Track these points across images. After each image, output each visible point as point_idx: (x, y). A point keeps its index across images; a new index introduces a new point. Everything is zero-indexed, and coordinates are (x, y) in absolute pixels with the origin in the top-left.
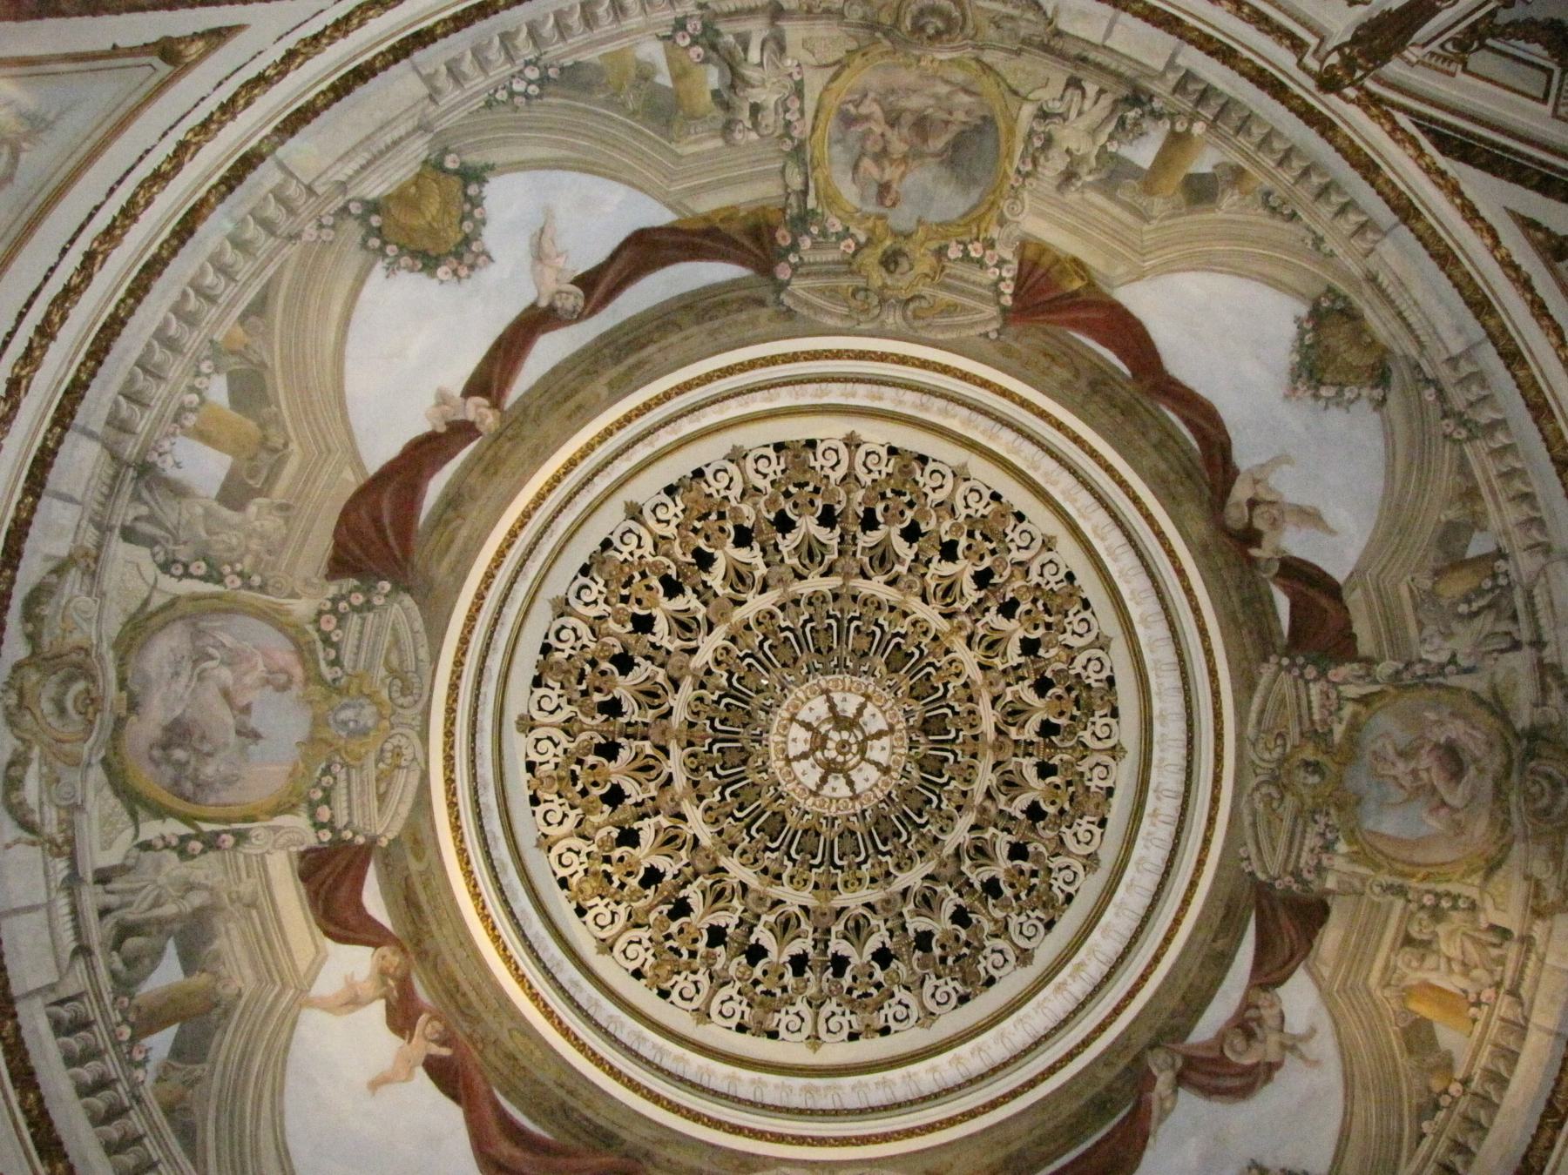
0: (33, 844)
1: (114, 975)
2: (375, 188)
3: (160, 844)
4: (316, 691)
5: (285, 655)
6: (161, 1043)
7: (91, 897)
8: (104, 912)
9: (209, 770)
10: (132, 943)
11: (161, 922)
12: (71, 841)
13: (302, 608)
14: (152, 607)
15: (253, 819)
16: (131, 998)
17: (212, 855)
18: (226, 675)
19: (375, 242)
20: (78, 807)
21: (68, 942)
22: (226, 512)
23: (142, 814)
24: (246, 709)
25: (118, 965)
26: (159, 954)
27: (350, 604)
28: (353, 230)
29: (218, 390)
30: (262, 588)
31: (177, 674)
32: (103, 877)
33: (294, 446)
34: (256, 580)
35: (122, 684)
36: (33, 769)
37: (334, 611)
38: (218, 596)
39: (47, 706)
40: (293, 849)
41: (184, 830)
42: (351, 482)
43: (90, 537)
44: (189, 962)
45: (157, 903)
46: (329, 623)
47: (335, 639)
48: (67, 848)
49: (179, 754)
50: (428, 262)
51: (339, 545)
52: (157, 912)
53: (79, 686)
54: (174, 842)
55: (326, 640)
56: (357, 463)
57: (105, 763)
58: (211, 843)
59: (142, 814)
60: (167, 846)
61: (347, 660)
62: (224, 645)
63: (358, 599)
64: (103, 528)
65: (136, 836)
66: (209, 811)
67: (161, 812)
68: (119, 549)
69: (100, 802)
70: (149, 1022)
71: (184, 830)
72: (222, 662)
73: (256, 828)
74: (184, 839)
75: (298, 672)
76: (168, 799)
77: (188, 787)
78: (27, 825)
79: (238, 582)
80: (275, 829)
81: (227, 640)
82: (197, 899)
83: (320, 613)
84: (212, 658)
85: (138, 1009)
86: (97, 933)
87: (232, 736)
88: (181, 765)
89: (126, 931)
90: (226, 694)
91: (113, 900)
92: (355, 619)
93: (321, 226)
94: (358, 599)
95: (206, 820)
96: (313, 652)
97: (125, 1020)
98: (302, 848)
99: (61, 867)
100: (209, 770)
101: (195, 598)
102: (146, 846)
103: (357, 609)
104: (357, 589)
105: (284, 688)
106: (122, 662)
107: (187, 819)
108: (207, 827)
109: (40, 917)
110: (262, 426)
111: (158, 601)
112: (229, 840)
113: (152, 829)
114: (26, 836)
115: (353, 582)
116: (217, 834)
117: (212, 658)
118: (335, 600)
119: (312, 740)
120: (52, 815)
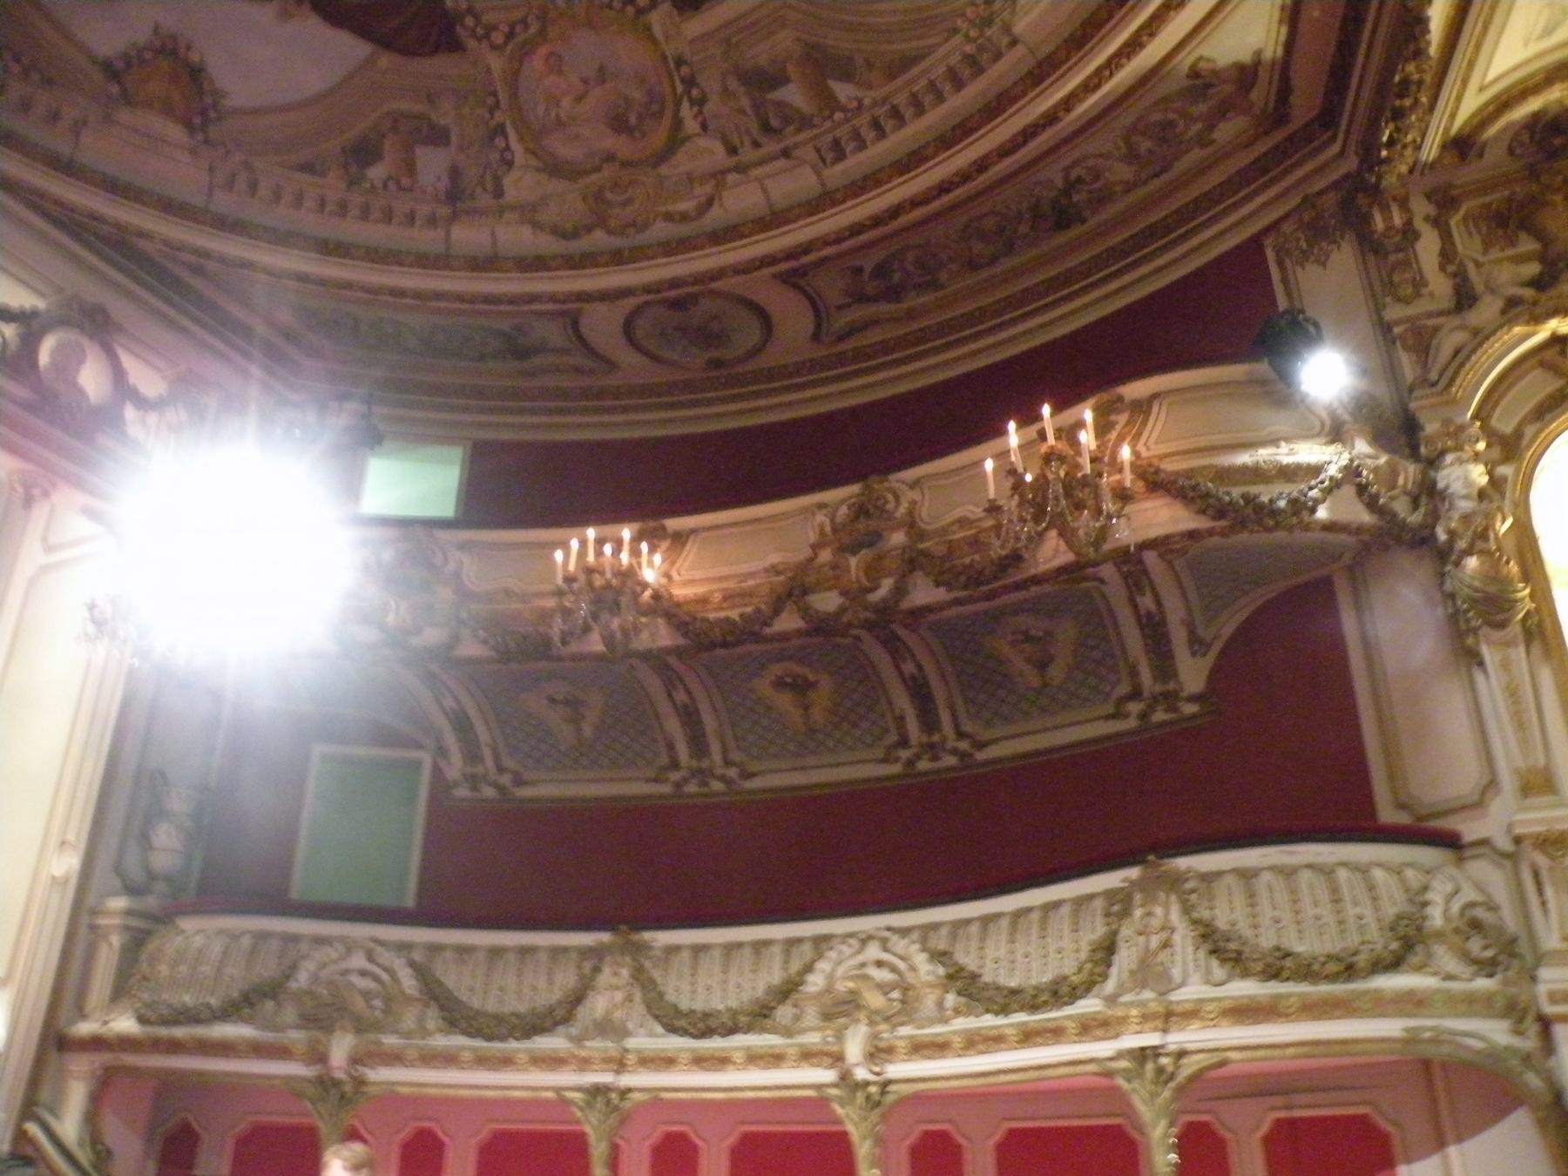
0: (720, 199)
1: (799, 130)
2: (176, 132)
3: (700, 119)
4: (552, 32)
5: (536, 63)
6: (843, 91)
7: (748, 154)
8: (756, 145)
9: (637, 95)
10: (774, 122)
11: (756, 107)
12: (713, 175)
13: (496, 63)
14: (541, 165)
15: (664, 58)
16: (813, 115)
17: (700, 79)
18: (566, 102)
19: (213, 114)
20: (690, 178)
21: (781, 163)
22: (454, 138)
23: (681, 135)
24: (585, 81)
25: (791, 128)
26: (780, 105)
27: (476, 25)
28: (213, 132)
29: (376, 173)
30: (494, 94)
31: (577, 136)
32: (732, 150)
33: (385, 108)
34: (490, 100)
35: (598, 169)
36: (670, 208)
37: (487, 36)
38: (514, 124)
39: (629, 209)
40: (677, 19)
41: (686, 104)
42: (385, 60)
43: (508, 216)
44: (780, 80)
45: (742, 111)
46: (498, 38)
47: (506, 29)
48: (718, 176)
49: (633, 120)
50: (196, 73)
51: (435, 51)
52: (749, 111)
53: (609, 195)
54: (696, 109)
55: (510, 35)
56: (369, 62)
57: (655, 166)
58: (690, 82)
59: (681, 135)
60: (700, 112)
61: (517, 15)
62: (546, 110)
63: (469, 21)
64: (501, 211)
65: (698, 135)
66: (668, 90)
67: (678, 124)
68: (511, 193)
69: (682, 162)
70: (829, 102)
71: (686, 104)
72: (558, 105)
73: (670, 50)
74: (692, 102)
75: (543, 50)
76: (667, 121)
77: (655, 108)
78: (710, 203)
79: (498, 114)
80: (667, 37)
81: (540, 110)
82: (733, 84)
83: (493, 47)
84: (558, 116)
85: (820, 110)
86: (771, 147)
87: (608, 86)
88: (640, 118)
89: (767, 128)
90: (580, 98)
91: (747, 142)
92: (487, 18)
93: (228, 152)
94: (469, 21)
95: (674, 88)
96: (524, 43)
97: (830, 117)
98: (675, 12)
99: (732, 178)
100: (637, 95)
101: (521, 139)
102: (704, 127)
103: (477, 17)
104: (462, 24)
105: (560, 58)
106: (587, 173)
107: (678, 104)
108: (680, 88)
109: (768, 183)
110: (384, 136)
111: (533, 162)
112: (685, 70)
113: (691, 125)
114: (716, 202)
115: (459, 29)
116: (683, 81)
117: (558, 116)
118: (479, 39)
119: (590, 24)
120: (698, 190)
